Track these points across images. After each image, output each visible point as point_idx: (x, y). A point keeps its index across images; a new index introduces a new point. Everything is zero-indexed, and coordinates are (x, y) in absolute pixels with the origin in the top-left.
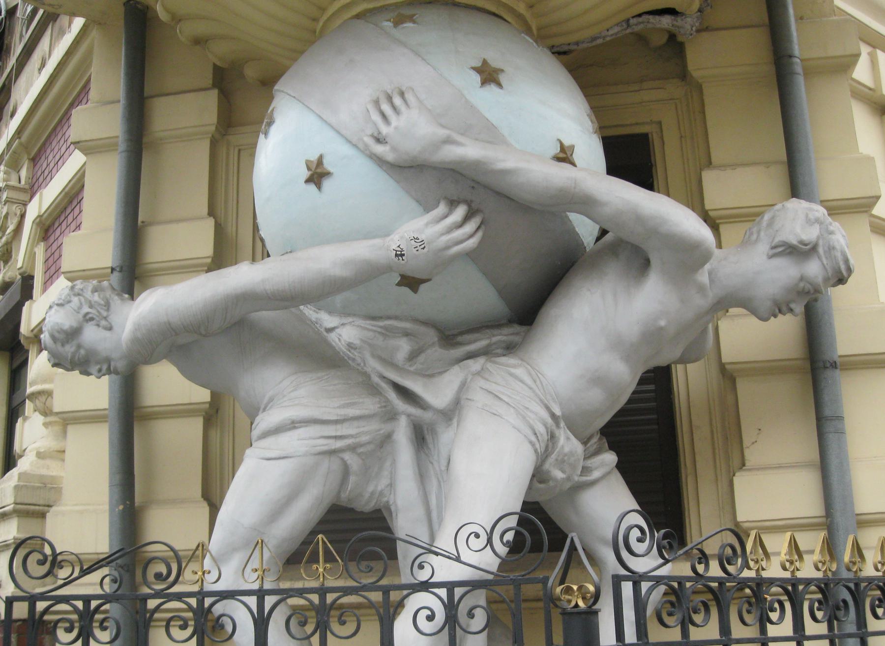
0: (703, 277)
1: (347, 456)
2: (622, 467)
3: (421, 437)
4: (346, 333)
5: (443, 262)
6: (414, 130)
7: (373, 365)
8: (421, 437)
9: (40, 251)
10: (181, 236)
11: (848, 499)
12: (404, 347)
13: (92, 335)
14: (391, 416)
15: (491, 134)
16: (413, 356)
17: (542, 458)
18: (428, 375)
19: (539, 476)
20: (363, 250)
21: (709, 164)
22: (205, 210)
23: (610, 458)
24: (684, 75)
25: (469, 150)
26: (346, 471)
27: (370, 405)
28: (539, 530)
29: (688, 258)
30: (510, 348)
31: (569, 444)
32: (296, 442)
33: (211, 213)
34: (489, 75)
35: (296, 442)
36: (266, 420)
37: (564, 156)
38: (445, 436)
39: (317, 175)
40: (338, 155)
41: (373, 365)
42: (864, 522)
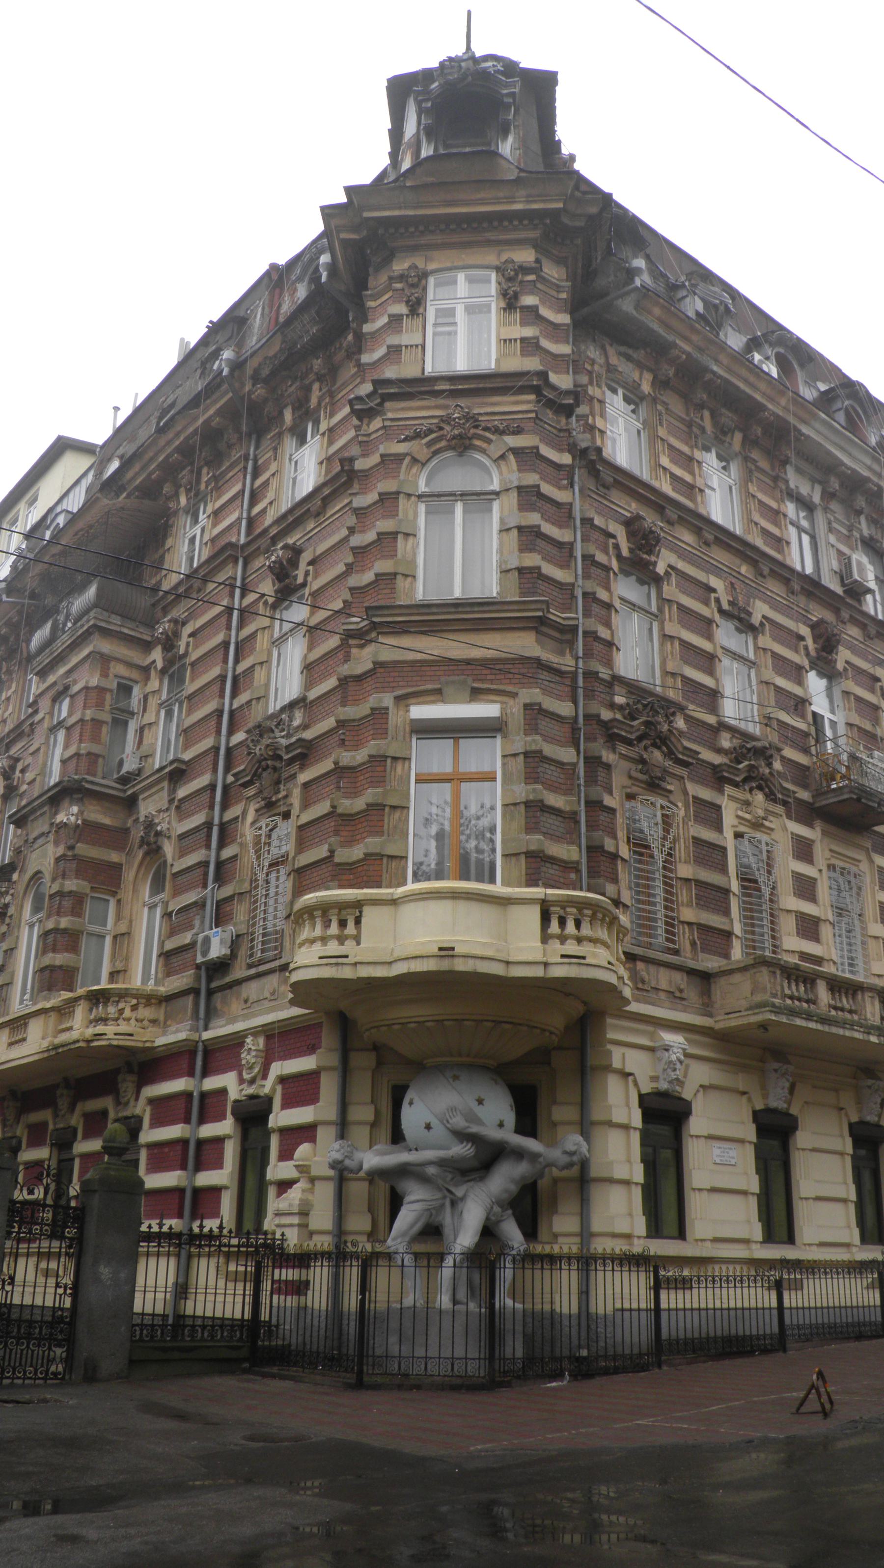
0: (541, 1159)
1: (434, 1212)
2: (514, 1214)
3: (453, 1204)
4: (431, 1170)
5: (463, 1159)
6: (459, 1122)
7: (440, 1182)
8: (453, 1204)
9: (279, 1088)
10: (362, 1113)
11: (589, 1226)
12: (450, 1176)
13: (347, 1162)
14: (444, 1197)
15: (479, 1122)
16: (452, 1179)
17: (488, 1214)
18: (456, 1185)
19: (488, 1219)
20: (442, 1154)
21: (554, 1102)
22: (369, 1100)
23: (510, 1212)
24: (549, 1064)
25: (474, 1129)
26: (431, 1215)
27: (439, 1195)
28: (488, 1232)
29: (534, 1157)
30: (482, 1179)
31: (497, 1209)
32: (417, 1206)
33: (372, 1102)
34: (480, 1102)
35: (417, 1206)
36: (407, 1199)
37: (501, 1125)
38: (460, 1205)
39: (428, 1127)
40: (435, 1123)
41: (440, 1182)
42: (593, 1235)
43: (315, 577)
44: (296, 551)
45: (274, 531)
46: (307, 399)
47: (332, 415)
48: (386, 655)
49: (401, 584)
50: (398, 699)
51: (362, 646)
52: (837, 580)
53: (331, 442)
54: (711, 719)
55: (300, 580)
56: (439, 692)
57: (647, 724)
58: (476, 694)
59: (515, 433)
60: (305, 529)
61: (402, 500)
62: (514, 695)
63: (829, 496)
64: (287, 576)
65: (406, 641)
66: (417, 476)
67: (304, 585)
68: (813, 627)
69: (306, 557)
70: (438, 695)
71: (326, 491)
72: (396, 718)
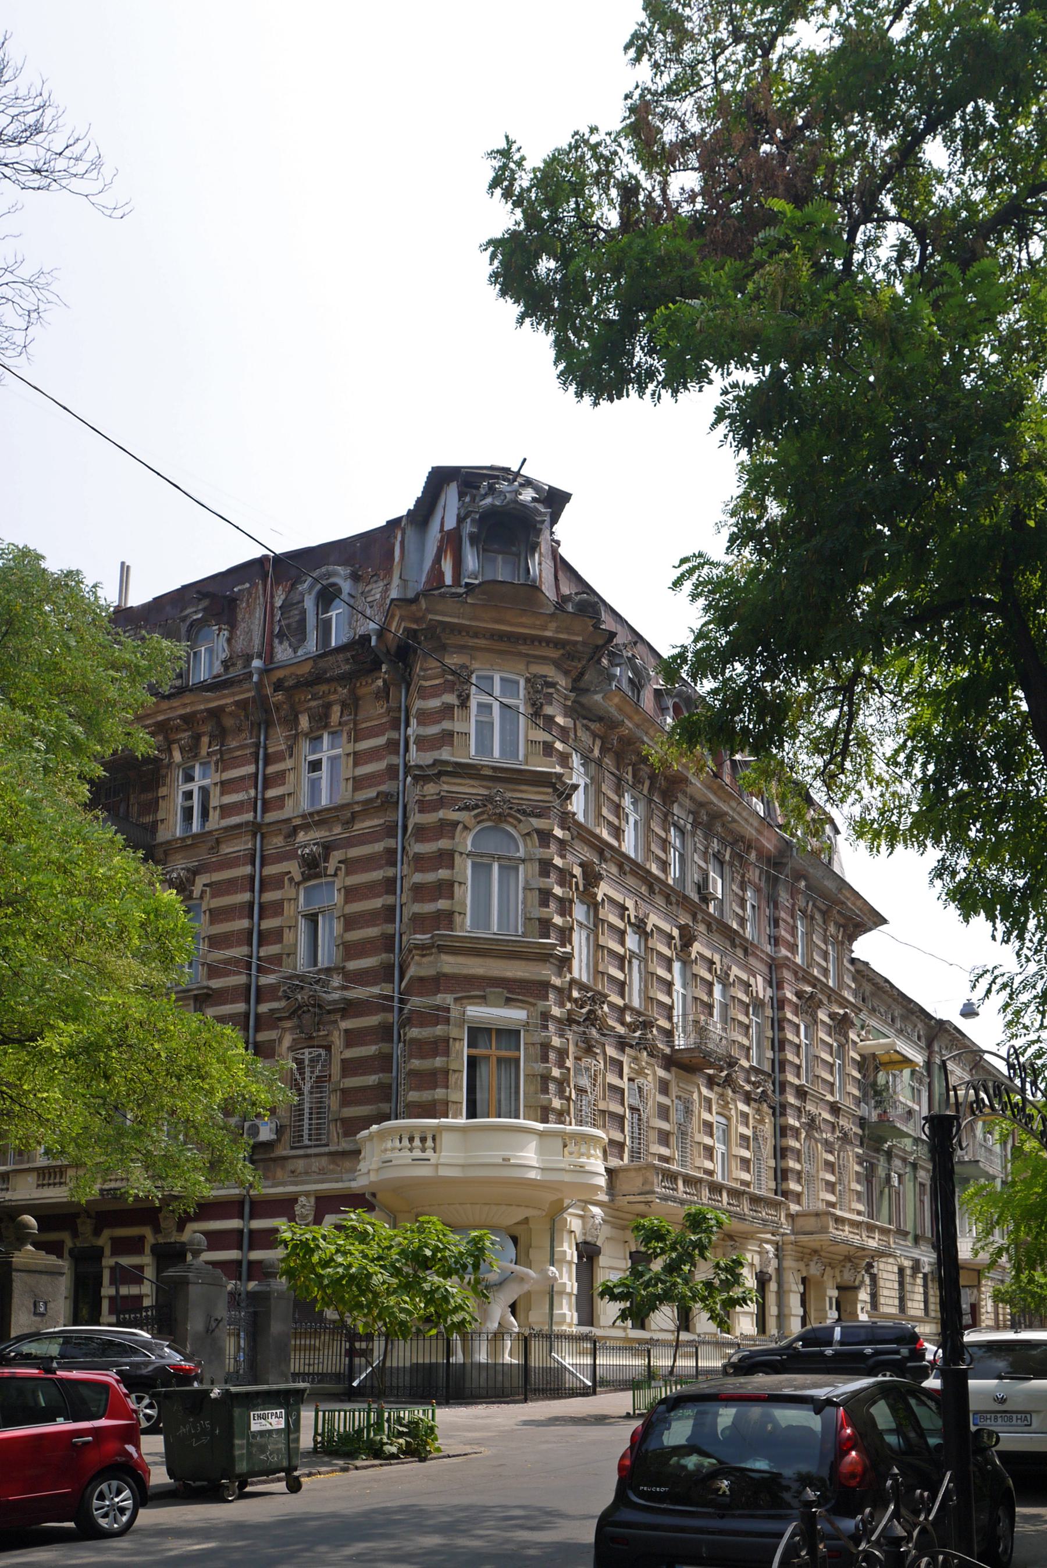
43: (347, 874)
44: (328, 848)
45: (298, 822)
46: (327, 716)
47: (355, 741)
48: (447, 969)
49: (458, 919)
50: (456, 999)
51: (423, 956)
52: (695, 889)
53: (356, 764)
54: (620, 1002)
55: (331, 871)
56: (484, 997)
57: (590, 1012)
58: (508, 1002)
59: (539, 816)
60: (330, 830)
61: (457, 856)
62: (534, 1005)
63: (695, 824)
64: (317, 866)
65: (460, 959)
66: (465, 838)
67: (335, 875)
68: (681, 928)
69: (336, 856)
70: (483, 1000)
71: (357, 808)
72: (454, 1014)
